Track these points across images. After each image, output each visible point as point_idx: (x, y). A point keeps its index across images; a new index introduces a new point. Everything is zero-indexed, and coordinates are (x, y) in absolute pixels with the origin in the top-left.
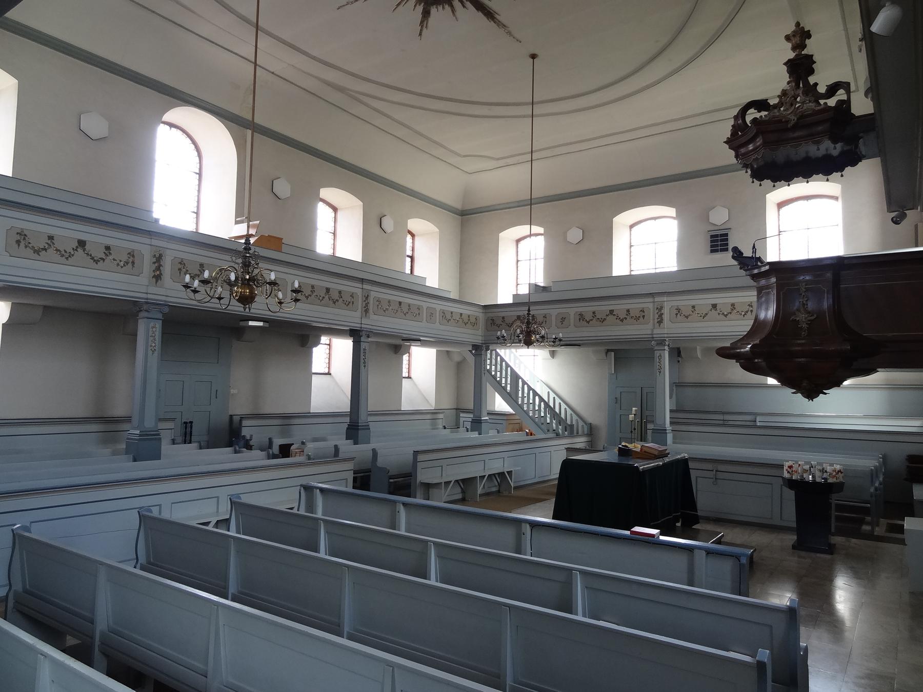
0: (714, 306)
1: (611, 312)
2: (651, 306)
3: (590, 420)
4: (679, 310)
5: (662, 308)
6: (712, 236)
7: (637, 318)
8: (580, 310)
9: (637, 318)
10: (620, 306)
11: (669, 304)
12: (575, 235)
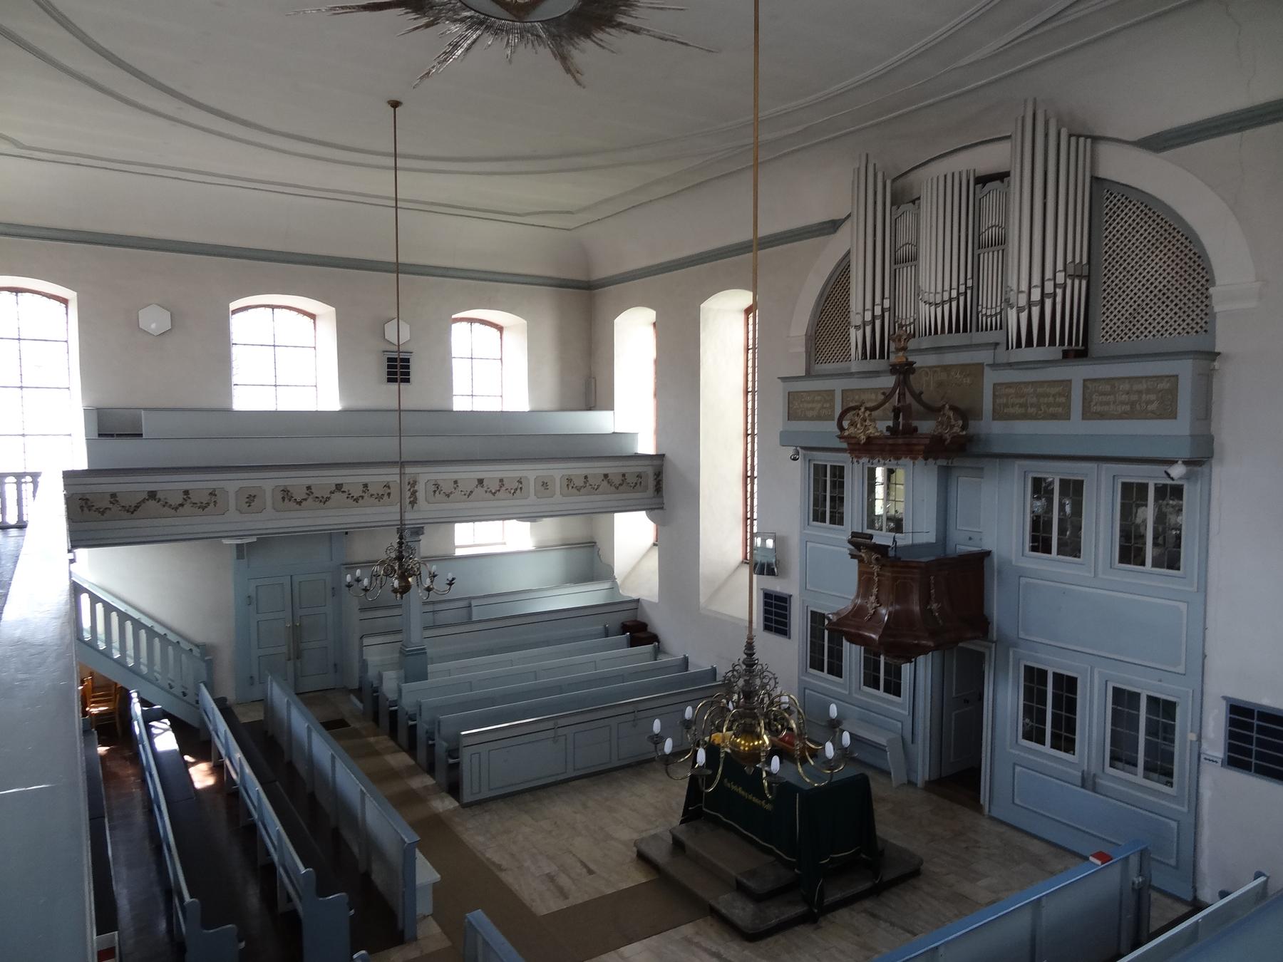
0: (481, 481)
1: (339, 487)
2: (397, 478)
3: (200, 638)
4: (437, 486)
5: (415, 482)
6: (390, 360)
7: (380, 497)
8: (282, 483)
9: (380, 497)
10: (353, 479)
11: (425, 476)
12: (154, 320)
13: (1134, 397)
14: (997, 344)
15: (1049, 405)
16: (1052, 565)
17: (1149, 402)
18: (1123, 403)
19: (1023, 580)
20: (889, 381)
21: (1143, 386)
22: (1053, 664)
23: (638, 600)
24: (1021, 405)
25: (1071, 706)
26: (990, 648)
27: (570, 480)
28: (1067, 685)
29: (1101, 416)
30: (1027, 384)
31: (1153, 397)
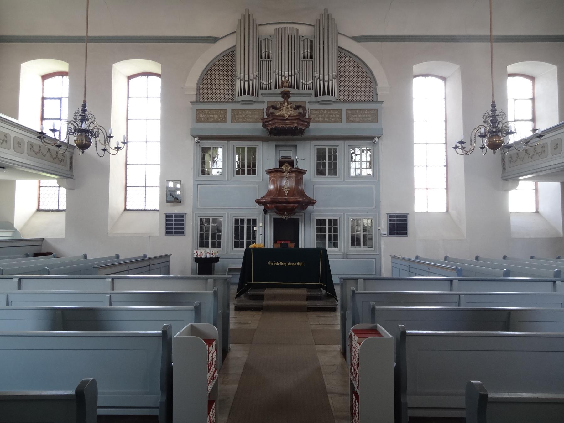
13: (364, 116)
14: (311, 94)
15: (333, 118)
16: (327, 178)
17: (368, 117)
18: (360, 117)
19: (315, 187)
20: (281, 99)
21: (366, 112)
22: (327, 216)
23: (43, 240)
24: (322, 118)
25: (336, 230)
26: (302, 215)
27: (32, 145)
28: (333, 223)
29: (353, 121)
30: (324, 110)
31: (369, 116)
